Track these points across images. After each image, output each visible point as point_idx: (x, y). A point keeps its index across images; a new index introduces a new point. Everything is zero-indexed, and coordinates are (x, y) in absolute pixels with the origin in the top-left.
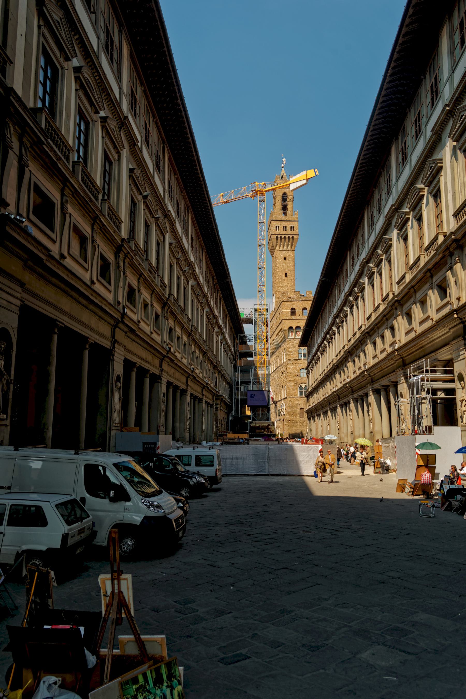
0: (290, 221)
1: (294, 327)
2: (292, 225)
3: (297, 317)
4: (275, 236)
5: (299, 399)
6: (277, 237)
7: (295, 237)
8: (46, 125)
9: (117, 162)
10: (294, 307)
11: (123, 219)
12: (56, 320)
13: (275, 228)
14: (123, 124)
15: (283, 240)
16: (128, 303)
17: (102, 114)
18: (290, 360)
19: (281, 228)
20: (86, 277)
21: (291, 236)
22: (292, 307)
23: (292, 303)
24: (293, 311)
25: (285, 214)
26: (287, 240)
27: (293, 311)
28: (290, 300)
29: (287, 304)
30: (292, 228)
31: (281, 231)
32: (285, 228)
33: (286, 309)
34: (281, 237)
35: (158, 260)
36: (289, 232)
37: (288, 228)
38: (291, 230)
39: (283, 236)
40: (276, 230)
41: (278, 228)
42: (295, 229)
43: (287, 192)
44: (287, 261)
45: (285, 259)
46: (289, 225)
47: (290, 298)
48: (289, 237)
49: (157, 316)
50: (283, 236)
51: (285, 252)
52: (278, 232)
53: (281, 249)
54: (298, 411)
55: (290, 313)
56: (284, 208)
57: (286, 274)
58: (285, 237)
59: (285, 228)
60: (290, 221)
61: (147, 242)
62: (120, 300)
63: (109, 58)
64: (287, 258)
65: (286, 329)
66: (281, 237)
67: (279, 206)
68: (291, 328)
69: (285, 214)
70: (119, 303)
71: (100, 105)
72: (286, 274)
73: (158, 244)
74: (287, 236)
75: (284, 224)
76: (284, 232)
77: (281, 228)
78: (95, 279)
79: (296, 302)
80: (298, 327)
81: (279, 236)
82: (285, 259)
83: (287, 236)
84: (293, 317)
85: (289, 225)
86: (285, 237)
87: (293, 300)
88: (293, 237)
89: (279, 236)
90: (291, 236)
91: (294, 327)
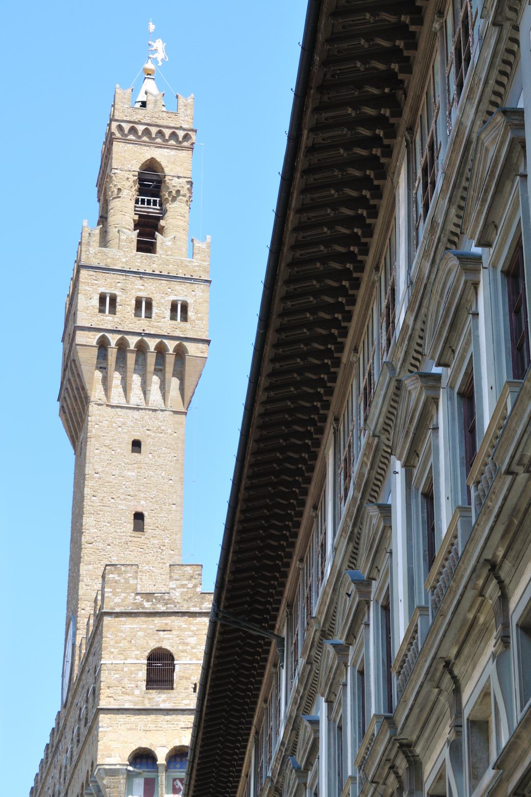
0: (169, 277)
2: (180, 298)
4: (92, 339)
6: (103, 345)
7: (192, 349)
10: (166, 645)
13: (96, 302)
19: (126, 306)
21: (171, 345)
22: (153, 645)
23: (158, 622)
25: (146, 246)
27: (160, 668)
30: (180, 310)
31: (125, 317)
32: (144, 306)
37: (161, 310)
38: (173, 318)
39: (133, 341)
40: (102, 311)
41: (108, 302)
42: (190, 314)
43: (164, 163)
44: (144, 456)
45: (136, 445)
46: (163, 296)
47: (148, 596)
50: (133, 341)
51: (136, 414)
52: (107, 321)
55: (142, 675)
56: (148, 231)
57: (139, 517)
59: (144, 306)
60: (169, 277)
68: (143, 757)
69: (146, 246)
72: (139, 517)
76: (142, 324)
77: (126, 306)
81: (113, 339)
82: (136, 445)
83: (152, 344)
84: (161, 699)
86: (141, 348)
87: (161, 608)
88: (180, 353)
89: (113, 339)
90: (171, 345)
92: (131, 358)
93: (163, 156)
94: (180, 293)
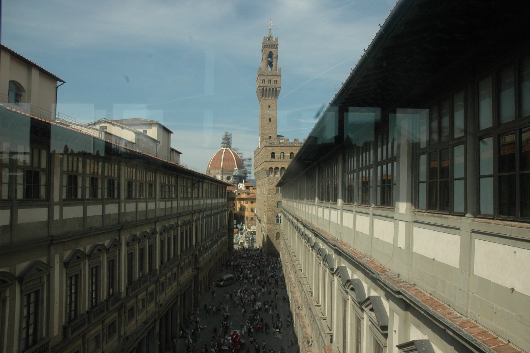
1: (274, 168)
3: (276, 159)
5: (276, 225)
6: (263, 89)
7: (278, 89)
15: (268, 91)
18: (270, 194)
19: (267, 82)
24: (273, 155)
26: (271, 91)
27: (273, 155)
28: (272, 145)
29: (269, 148)
30: (276, 81)
31: (267, 84)
32: (270, 81)
33: (268, 153)
34: (266, 89)
36: (273, 85)
37: (273, 82)
39: (268, 88)
41: (264, 81)
44: (271, 108)
45: (269, 106)
48: (273, 89)
50: (268, 88)
52: (264, 85)
53: (267, 98)
54: (275, 234)
57: (270, 119)
58: (270, 89)
59: (270, 81)
64: (271, 106)
65: (267, 169)
66: (266, 89)
67: (265, 62)
68: (271, 168)
72: (270, 119)
74: (271, 89)
75: (269, 78)
76: (269, 85)
77: (267, 82)
79: (276, 148)
80: (277, 168)
82: (269, 106)
83: (271, 89)
84: (273, 160)
85: (273, 79)
88: (276, 89)
91: (274, 168)
92: (268, 91)
93: (272, 50)
94: (276, 78)
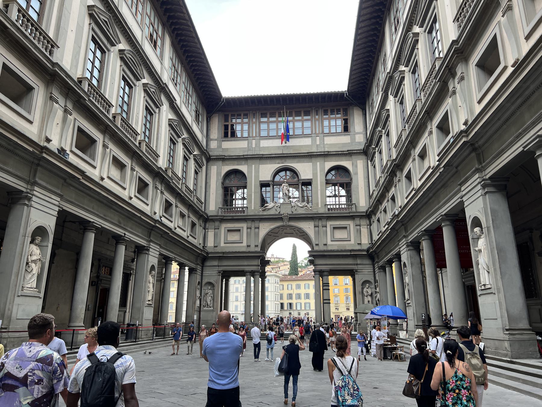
8: (88, 89)
9: (157, 115)
11: (161, 154)
12: (93, 222)
14: (162, 88)
16: (164, 214)
17: (144, 81)
20: (124, 194)
35: (195, 184)
49: (193, 225)
61: (185, 172)
62: (157, 211)
63: (153, 46)
70: (155, 213)
71: (142, 76)
73: (196, 173)
78: (133, 196)
